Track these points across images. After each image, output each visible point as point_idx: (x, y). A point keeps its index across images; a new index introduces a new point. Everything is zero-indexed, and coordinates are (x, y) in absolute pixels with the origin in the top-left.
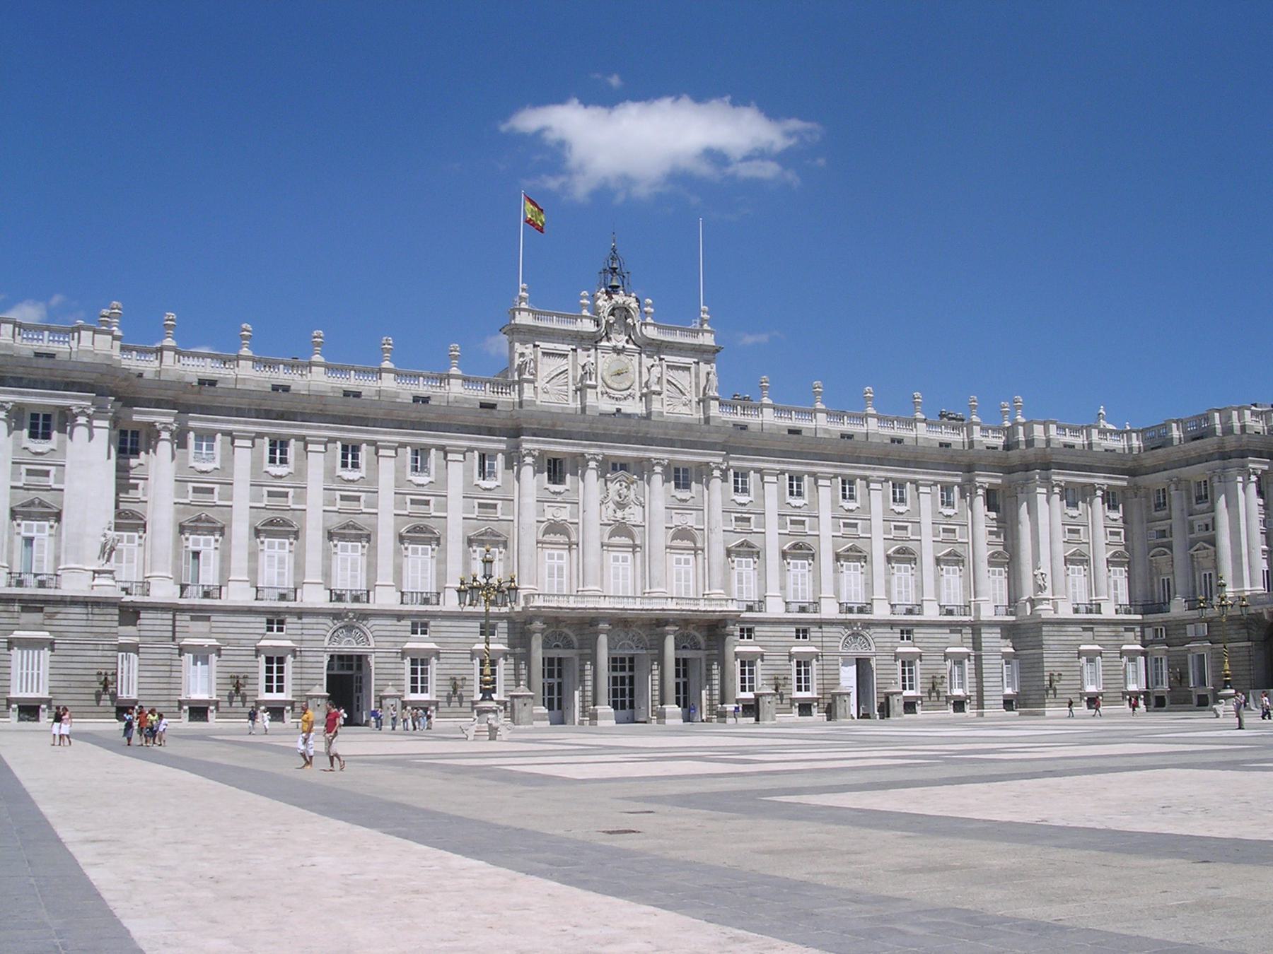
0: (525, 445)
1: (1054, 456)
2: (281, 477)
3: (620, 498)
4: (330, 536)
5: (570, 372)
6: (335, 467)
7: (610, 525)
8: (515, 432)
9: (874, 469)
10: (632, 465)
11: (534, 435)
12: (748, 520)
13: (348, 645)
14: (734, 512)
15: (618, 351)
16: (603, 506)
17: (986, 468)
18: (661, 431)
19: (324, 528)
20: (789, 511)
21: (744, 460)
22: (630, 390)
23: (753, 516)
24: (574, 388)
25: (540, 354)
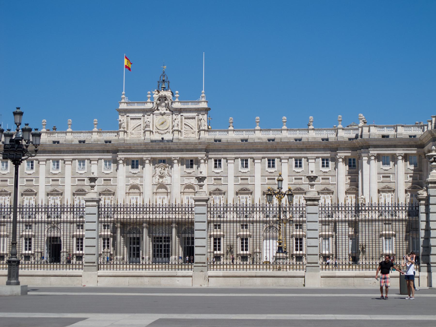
0: (120, 156)
1: (371, 142)
2: (31, 174)
3: (160, 173)
4: (48, 195)
5: (142, 125)
6: (50, 169)
7: (157, 185)
8: (115, 151)
9: (284, 154)
10: (167, 160)
11: (123, 152)
12: (220, 179)
13: (54, 234)
14: (213, 176)
15: (162, 115)
16: (154, 178)
17: (344, 149)
18: (176, 146)
19: (45, 191)
20: (240, 174)
21: (217, 154)
22: (168, 130)
23: (222, 178)
24: (143, 131)
25: (129, 119)
